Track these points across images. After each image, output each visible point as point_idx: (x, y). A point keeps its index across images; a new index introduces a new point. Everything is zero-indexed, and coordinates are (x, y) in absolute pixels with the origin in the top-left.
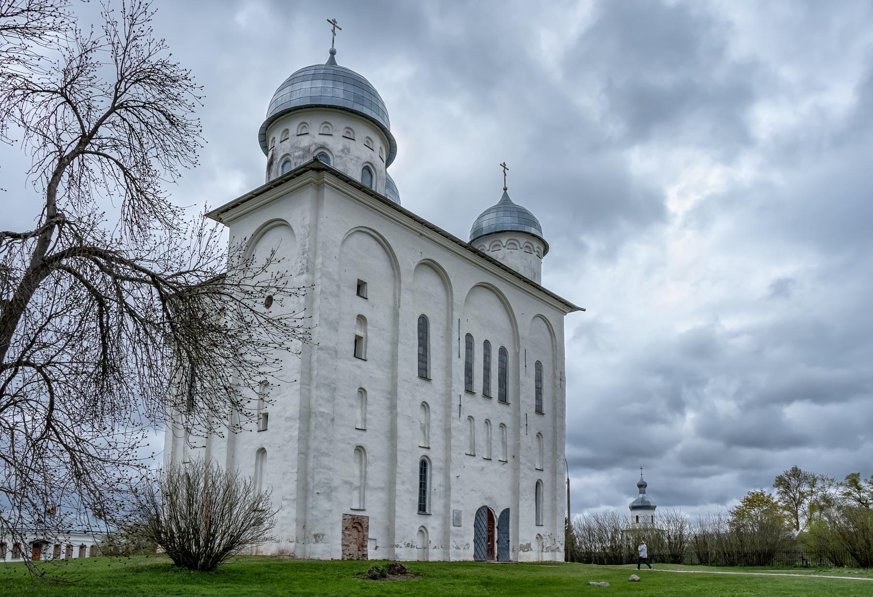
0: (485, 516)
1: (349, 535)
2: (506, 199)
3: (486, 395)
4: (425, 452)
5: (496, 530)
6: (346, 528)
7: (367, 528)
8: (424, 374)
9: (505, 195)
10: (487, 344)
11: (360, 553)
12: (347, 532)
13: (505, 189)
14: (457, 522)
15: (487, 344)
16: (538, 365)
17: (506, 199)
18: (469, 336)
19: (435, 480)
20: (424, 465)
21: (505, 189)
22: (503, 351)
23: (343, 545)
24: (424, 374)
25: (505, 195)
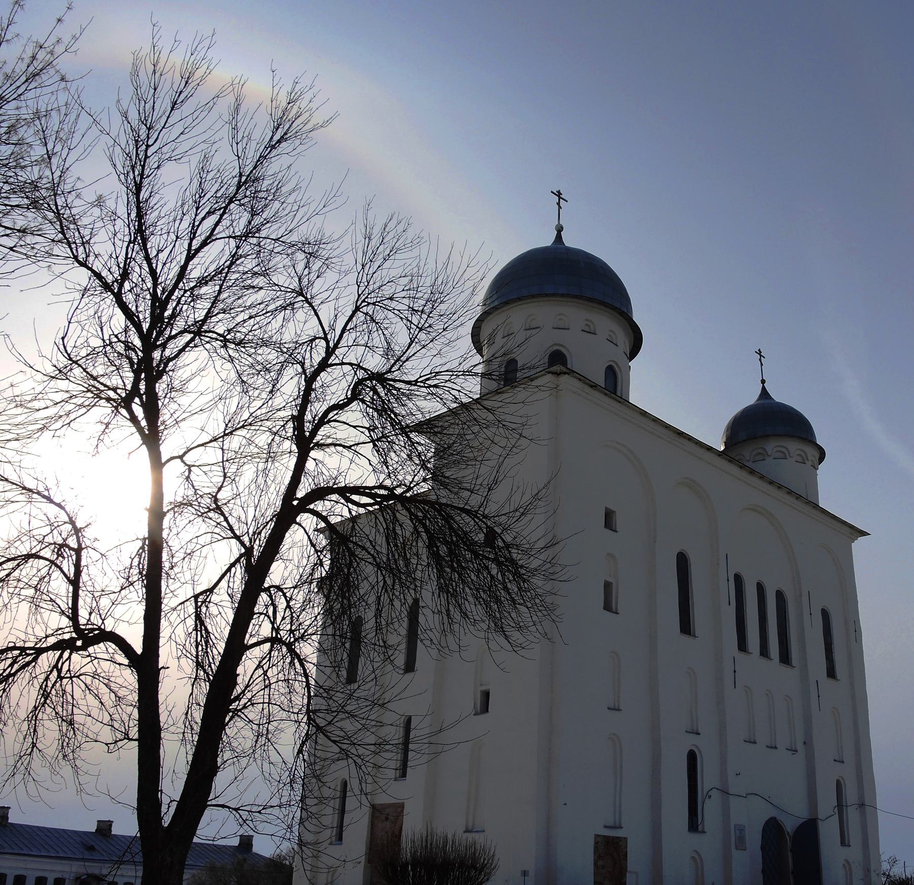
0: (772, 828)
1: (603, 867)
2: (764, 394)
3: (764, 652)
5: (790, 854)
8: (686, 627)
9: (764, 388)
10: (760, 588)
12: (600, 863)
13: (763, 382)
14: (741, 843)
15: (760, 588)
17: (764, 394)
18: (738, 579)
19: (708, 779)
20: (692, 758)
21: (763, 382)
22: (780, 595)
24: (686, 627)
25: (764, 388)
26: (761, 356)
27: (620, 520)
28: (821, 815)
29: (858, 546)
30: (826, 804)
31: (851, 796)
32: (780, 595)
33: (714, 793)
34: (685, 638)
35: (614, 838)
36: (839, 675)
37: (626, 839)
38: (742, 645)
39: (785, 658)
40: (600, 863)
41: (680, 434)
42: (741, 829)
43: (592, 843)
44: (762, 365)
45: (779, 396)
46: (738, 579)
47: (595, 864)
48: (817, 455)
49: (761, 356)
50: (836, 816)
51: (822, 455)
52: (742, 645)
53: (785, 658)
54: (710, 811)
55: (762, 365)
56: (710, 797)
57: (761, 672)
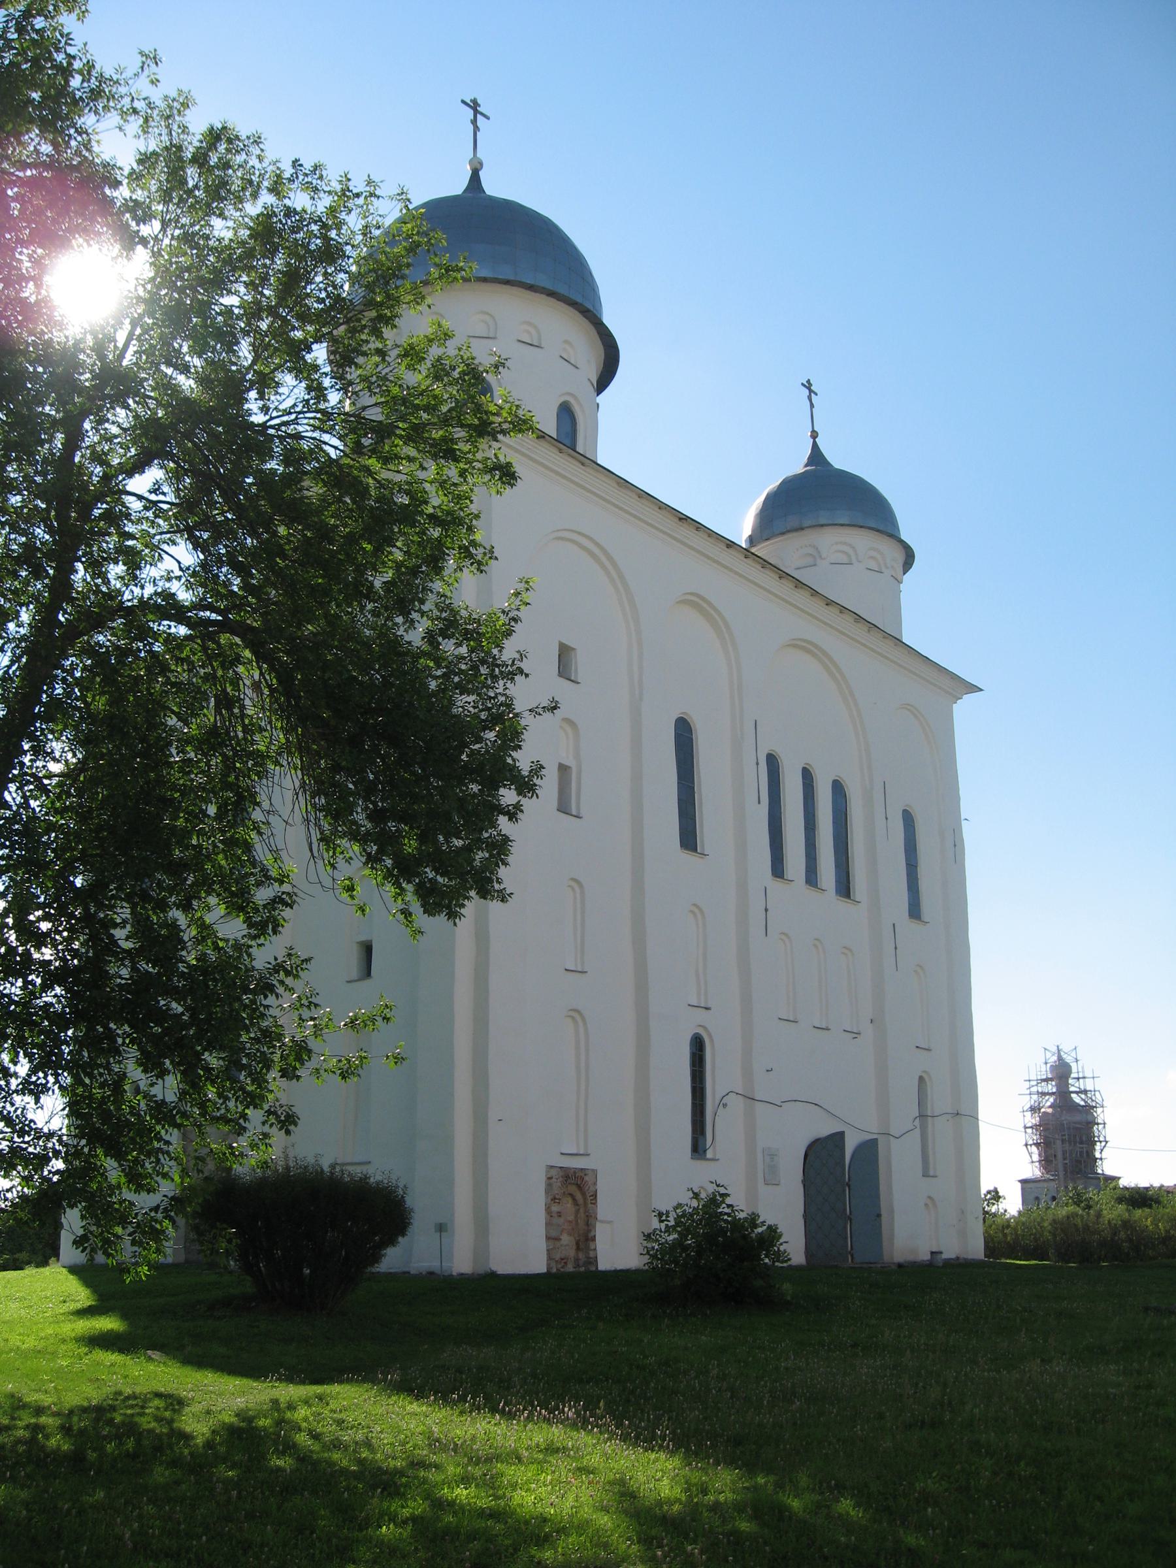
1: (559, 1214)
2: (816, 457)
4: (700, 1016)
6: (554, 1199)
7: (595, 1196)
8: (689, 839)
10: (807, 776)
11: (581, 1255)
12: (555, 1208)
13: (814, 435)
15: (807, 776)
17: (816, 457)
20: (698, 1046)
21: (814, 435)
22: (838, 788)
23: (548, 1238)
24: (689, 839)
26: (811, 391)
27: (582, 664)
29: (964, 709)
30: (904, 1113)
31: (939, 1102)
32: (838, 788)
34: (687, 857)
35: (576, 1170)
36: (926, 915)
37: (595, 1172)
38: (778, 869)
39: (845, 888)
41: (684, 519)
42: (771, 1155)
43: (543, 1178)
44: (812, 406)
45: (839, 459)
47: (548, 1209)
48: (900, 557)
49: (811, 391)
50: (918, 1131)
51: (909, 558)
52: (778, 869)
53: (845, 888)
54: (726, 1126)
55: (812, 406)
56: (725, 1105)
57: (803, 907)
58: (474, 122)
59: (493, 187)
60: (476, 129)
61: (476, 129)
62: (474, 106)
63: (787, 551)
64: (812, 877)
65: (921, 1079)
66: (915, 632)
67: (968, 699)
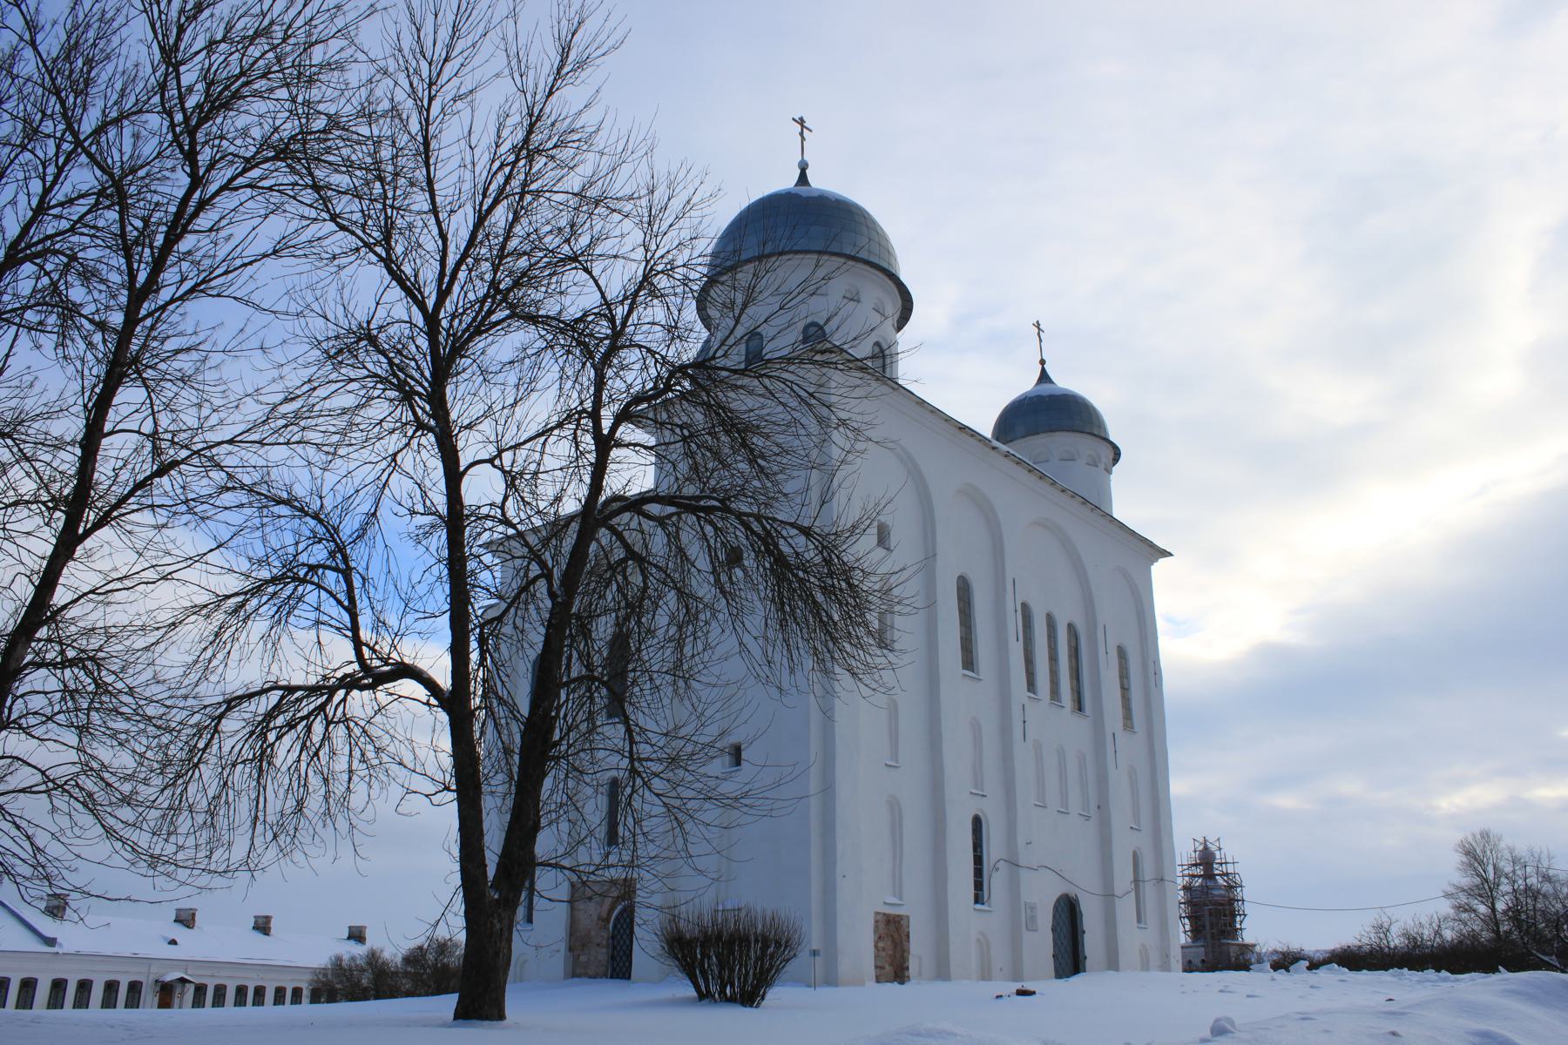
12: (881, 945)
13: (1043, 362)
16: (1122, 654)
19: (994, 849)
20: (977, 823)
21: (1043, 362)
22: (1071, 627)
23: (876, 967)
28: (1118, 891)
29: (1159, 569)
31: (1148, 871)
33: (1001, 865)
39: (1079, 706)
40: (881, 945)
41: (963, 428)
45: (1064, 381)
46: (1025, 607)
47: (876, 946)
48: (1111, 456)
53: (1079, 706)
54: (997, 883)
58: (802, 134)
59: (817, 182)
60: (803, 139)
61: (803, 139)
62: (801, 122)
63: (1027, 447)
64: (1055, 693)
65: (1135, 854)
66: (1117, 514)
67: (1162, 561)
